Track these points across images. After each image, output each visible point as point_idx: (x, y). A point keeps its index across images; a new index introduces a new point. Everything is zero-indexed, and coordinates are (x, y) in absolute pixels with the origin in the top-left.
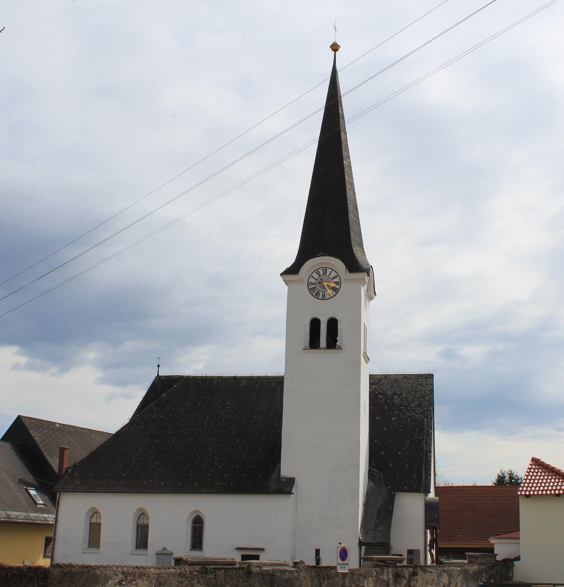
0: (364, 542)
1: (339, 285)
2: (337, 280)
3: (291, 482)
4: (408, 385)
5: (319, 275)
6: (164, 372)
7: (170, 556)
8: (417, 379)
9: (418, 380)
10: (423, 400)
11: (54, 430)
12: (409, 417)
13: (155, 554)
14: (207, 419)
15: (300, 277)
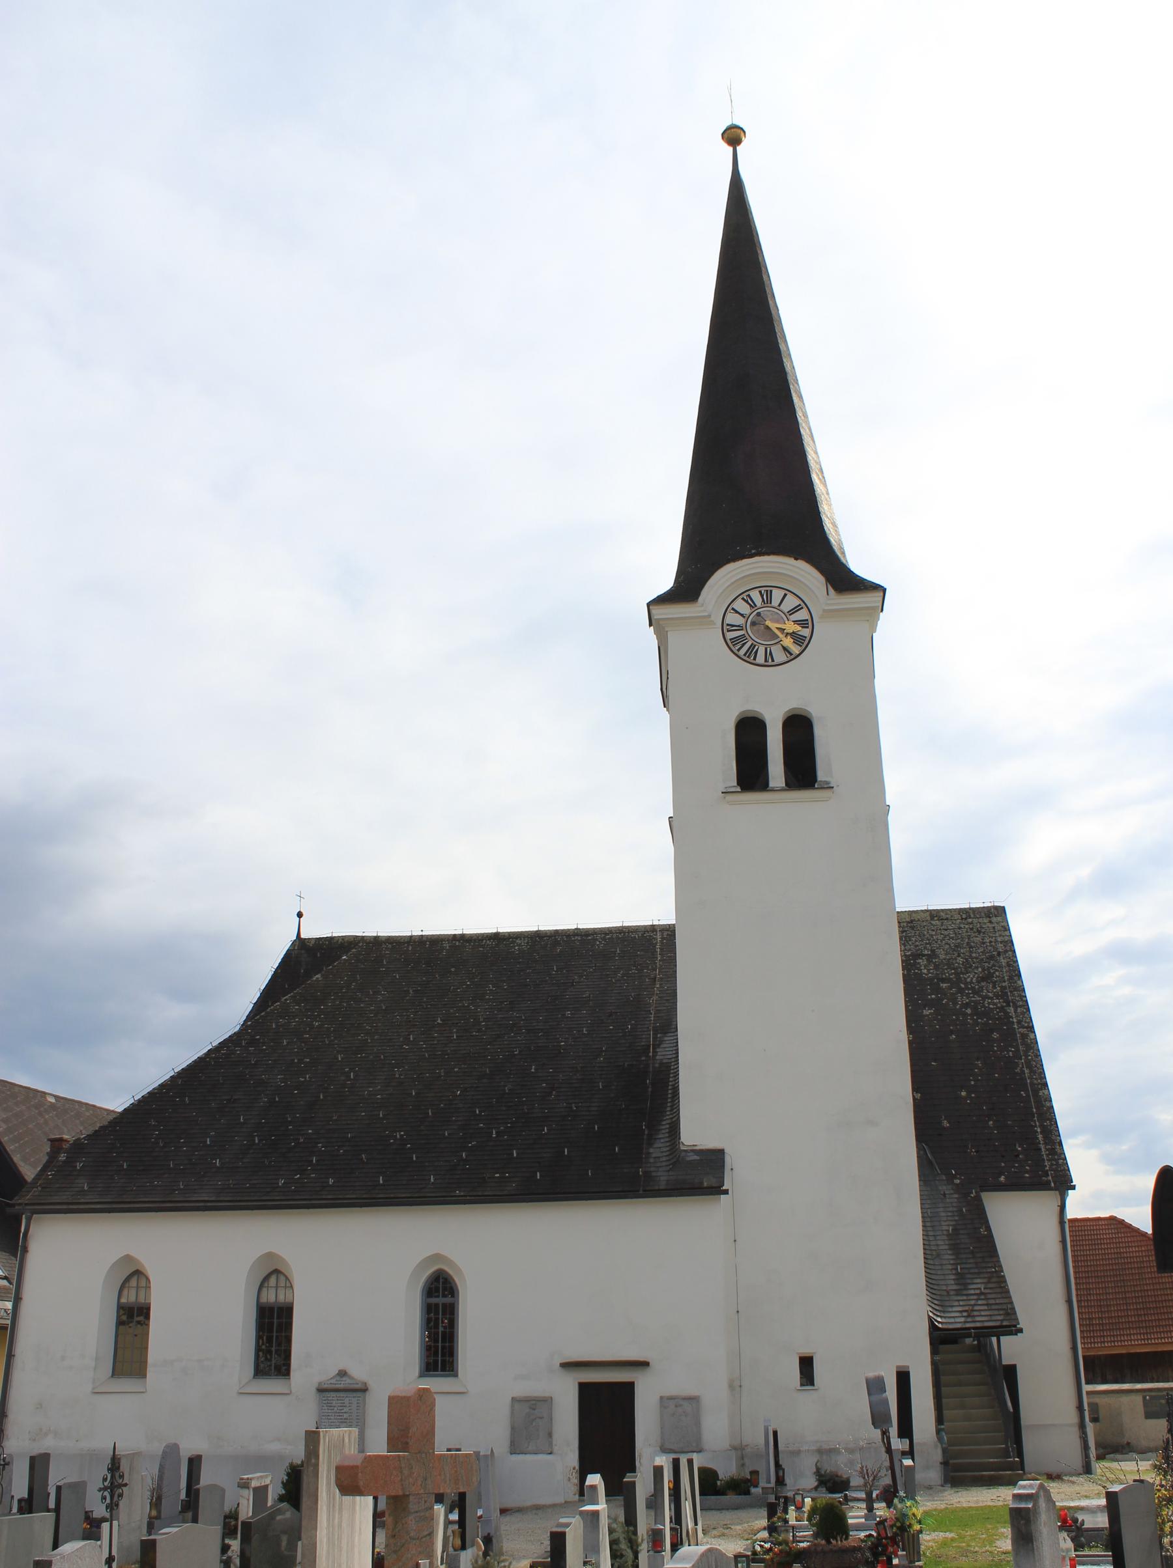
0: (945, 1326)
1: (808, 627)
2: (802, 615)
3: (714, 1160)
4: (946, 933)
5: (753, 605)
6: (314, 930)
7: (359, 1394)
8: (966, 919)
9: (970, 920)
10: (994, 965)
11: (42, 1109)
12: (967, 1005)
13: (314, 1390)
14: (438, 1023)
15: (702, 608)
